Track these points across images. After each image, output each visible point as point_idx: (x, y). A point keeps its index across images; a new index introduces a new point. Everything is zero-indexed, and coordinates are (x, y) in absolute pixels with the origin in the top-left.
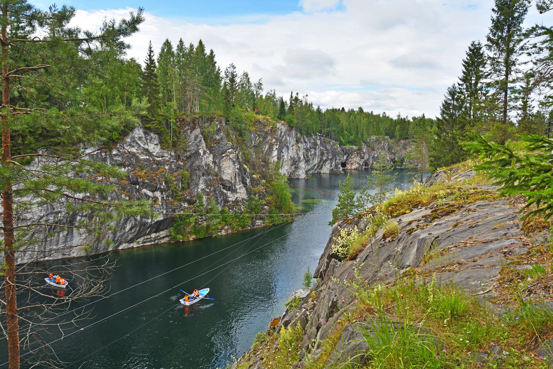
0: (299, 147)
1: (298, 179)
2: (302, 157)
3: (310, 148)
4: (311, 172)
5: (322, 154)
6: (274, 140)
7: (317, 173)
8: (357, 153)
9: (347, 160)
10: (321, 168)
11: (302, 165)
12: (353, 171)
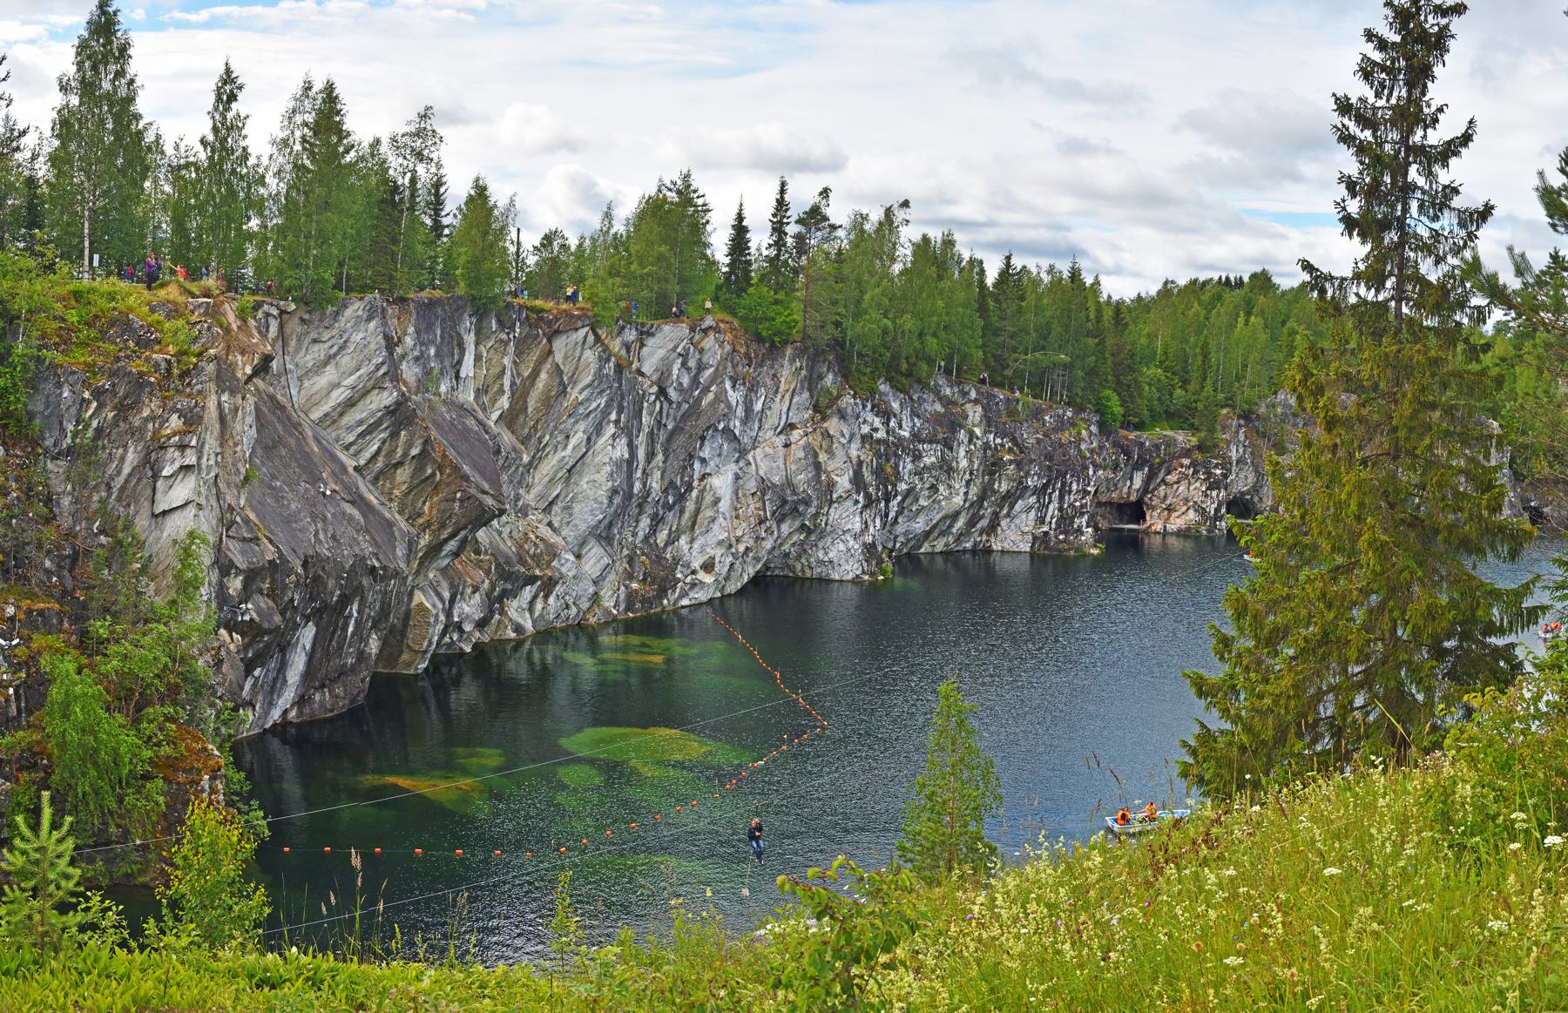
0: (827, 435)
1: (826, 581)
2: (843, 482)
3: (916, 437)
4: (940, 546)
5: (993, 467)
6: (175, 422)
7: (974, 551)
8: (1194, 464)
9: (1145, 490)
10: (993, 527)
11: (848, 517)
12: (1172, 540)
